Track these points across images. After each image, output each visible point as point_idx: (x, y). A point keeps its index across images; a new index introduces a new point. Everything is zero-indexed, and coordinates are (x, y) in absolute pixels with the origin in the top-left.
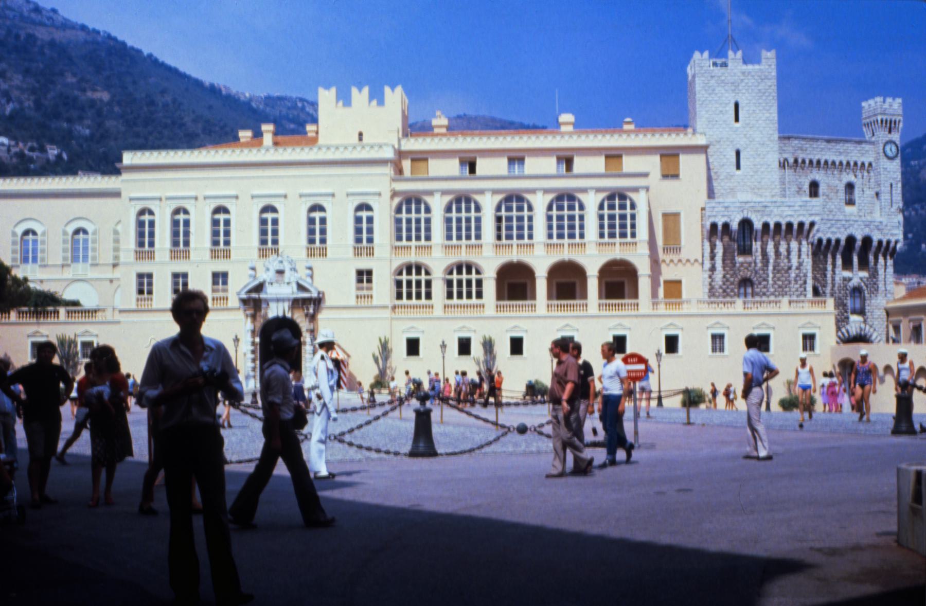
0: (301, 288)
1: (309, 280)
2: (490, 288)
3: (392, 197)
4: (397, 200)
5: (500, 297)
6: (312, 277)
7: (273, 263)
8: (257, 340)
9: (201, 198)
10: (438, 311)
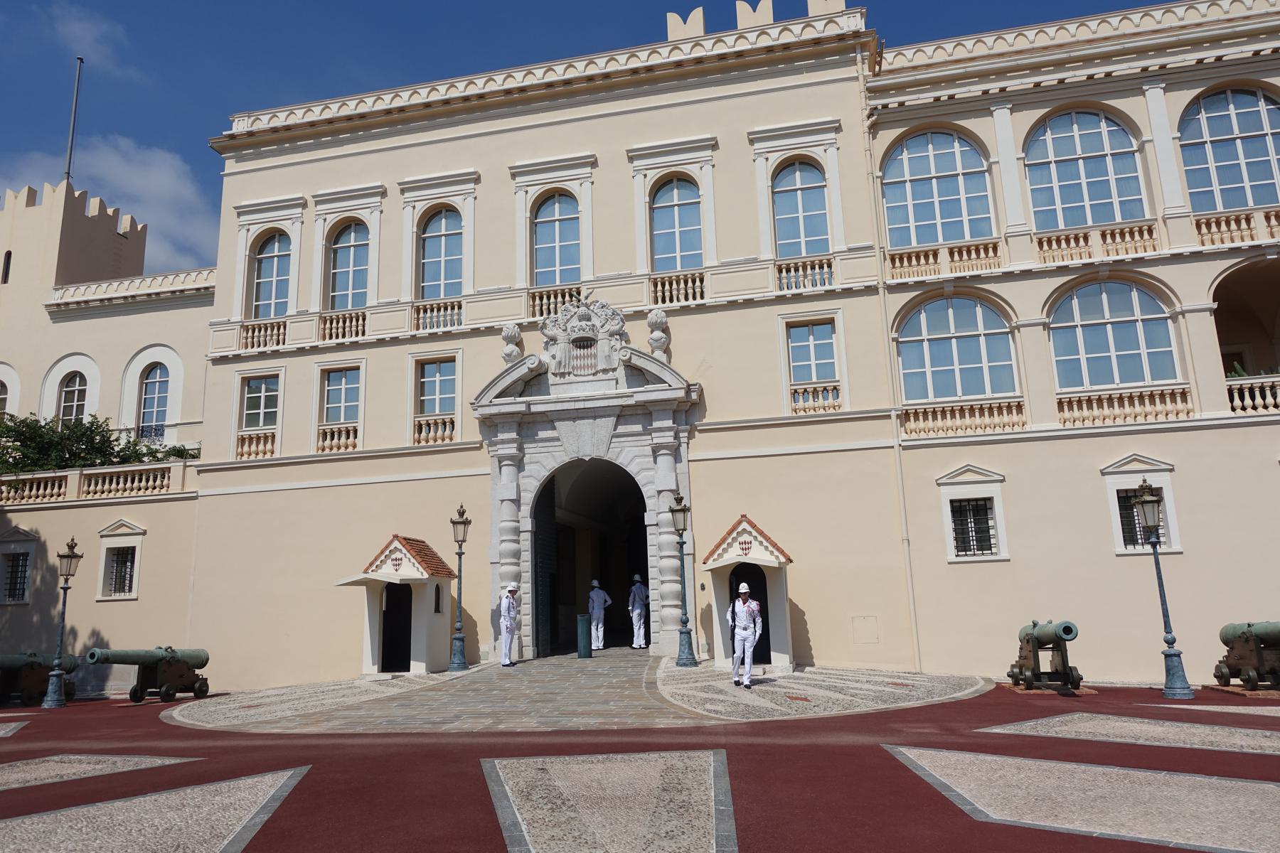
0: (637, 375)
1: (659, 355)
2: (1198, 343)
3: (874, 129)
4: (888, 136)
5: (1233, 362)
6: (667, 351)
7: (567, 322)
8: (527, 524)
9: (394, 191)
10: (1042, 416)
